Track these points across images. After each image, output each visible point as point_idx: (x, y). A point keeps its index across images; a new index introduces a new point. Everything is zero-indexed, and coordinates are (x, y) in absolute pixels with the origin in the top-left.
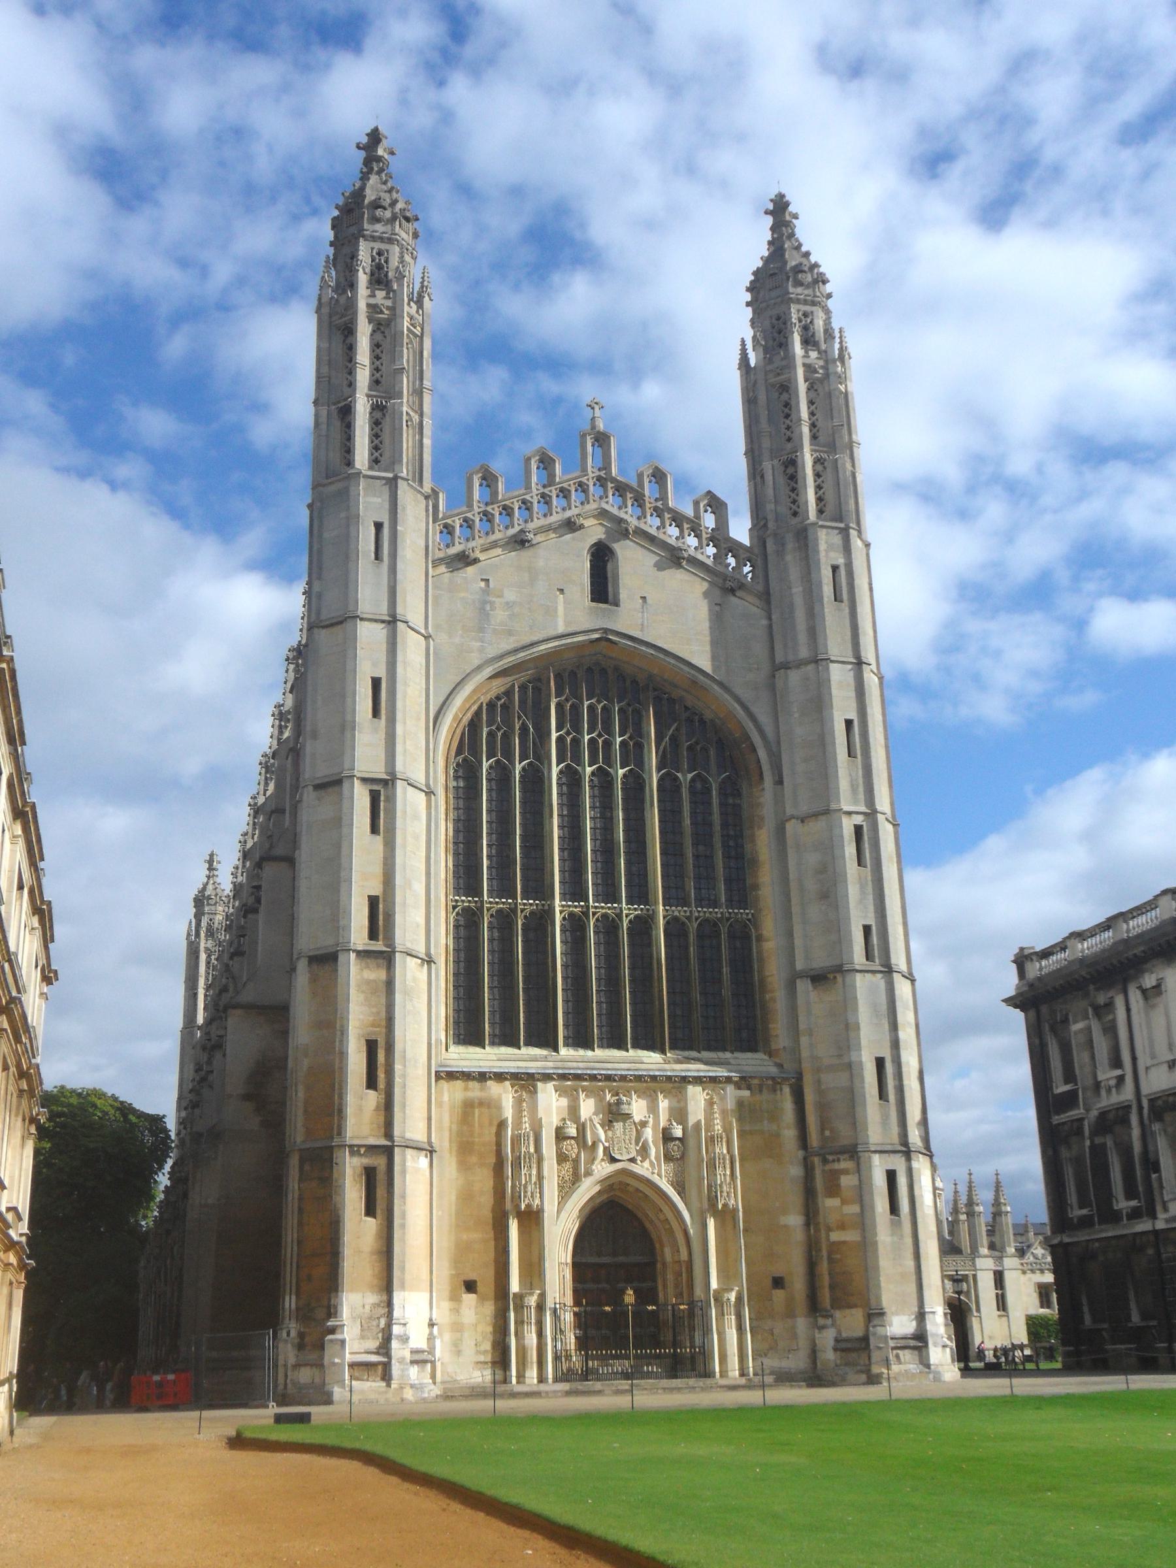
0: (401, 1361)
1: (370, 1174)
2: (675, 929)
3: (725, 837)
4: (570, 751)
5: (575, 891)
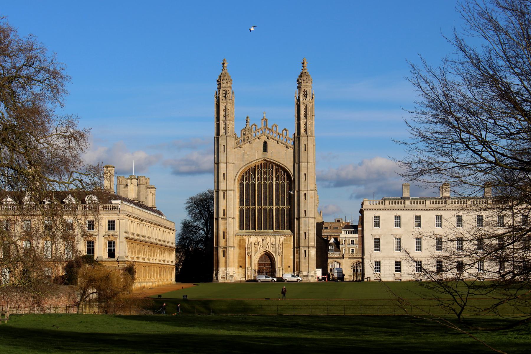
0: (228, 277)
1: (224, 251)
2: (277, 210)
4: (259, 179)
5: (260, 204)
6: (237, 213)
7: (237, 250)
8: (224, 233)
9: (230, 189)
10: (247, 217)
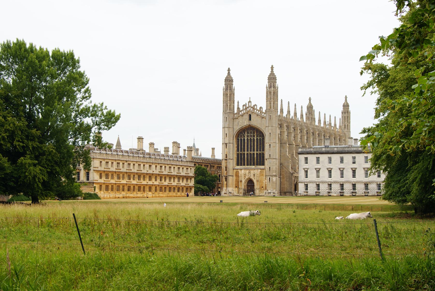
1: (226, 178)
2: (257, 154)
3: (263, 144)
4: (248, 136)
5: (248, 151)
6: (235, 156)
7: (235, 177)
8: (226, 167)
9: (230, 142)
10: (241, 159)
